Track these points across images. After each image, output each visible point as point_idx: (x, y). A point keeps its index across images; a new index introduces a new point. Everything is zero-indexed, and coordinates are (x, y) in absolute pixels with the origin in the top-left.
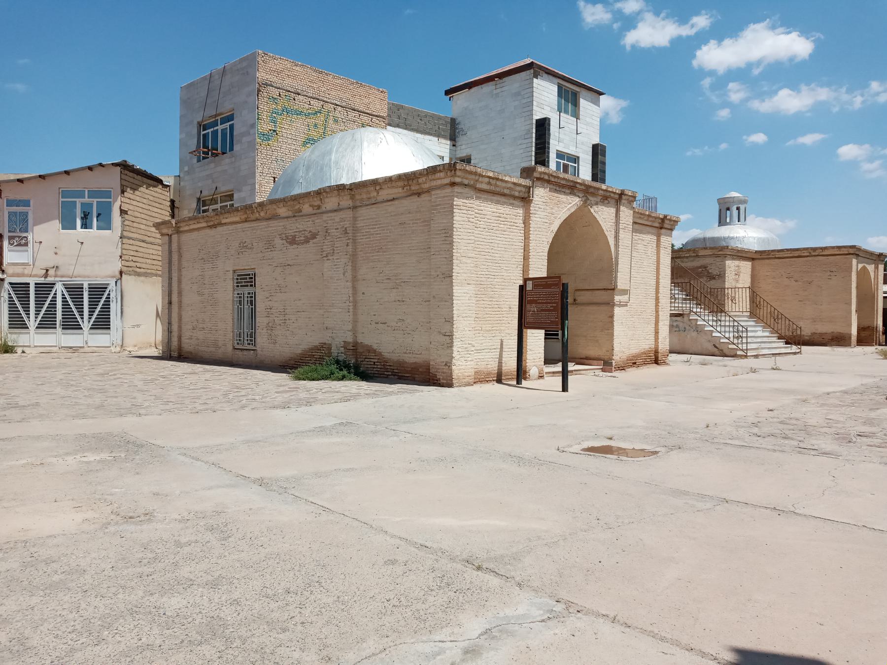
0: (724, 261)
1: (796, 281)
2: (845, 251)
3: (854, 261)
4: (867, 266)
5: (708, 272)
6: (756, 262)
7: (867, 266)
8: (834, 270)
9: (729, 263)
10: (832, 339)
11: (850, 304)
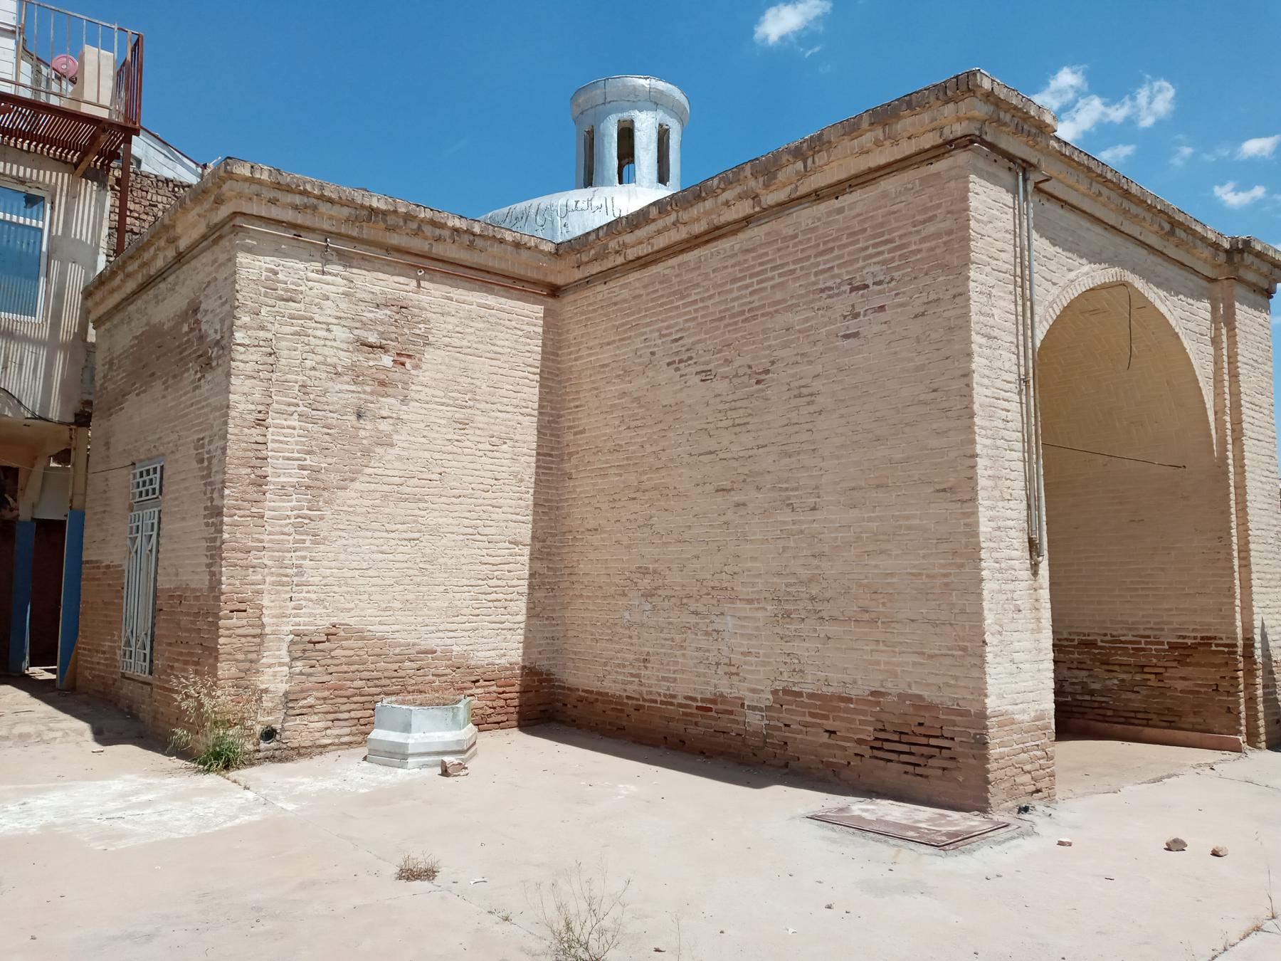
0: (231, 259)
1: (706, 375)
2: (917, 132)
3: (990, 204)
4: (1139, 283)
5: (201, 338)
6: (569, 305)
7: (1153, 294)
8: (872, 271)
9: (252, 266)
10: (878, 746)
11: (961, 491)
